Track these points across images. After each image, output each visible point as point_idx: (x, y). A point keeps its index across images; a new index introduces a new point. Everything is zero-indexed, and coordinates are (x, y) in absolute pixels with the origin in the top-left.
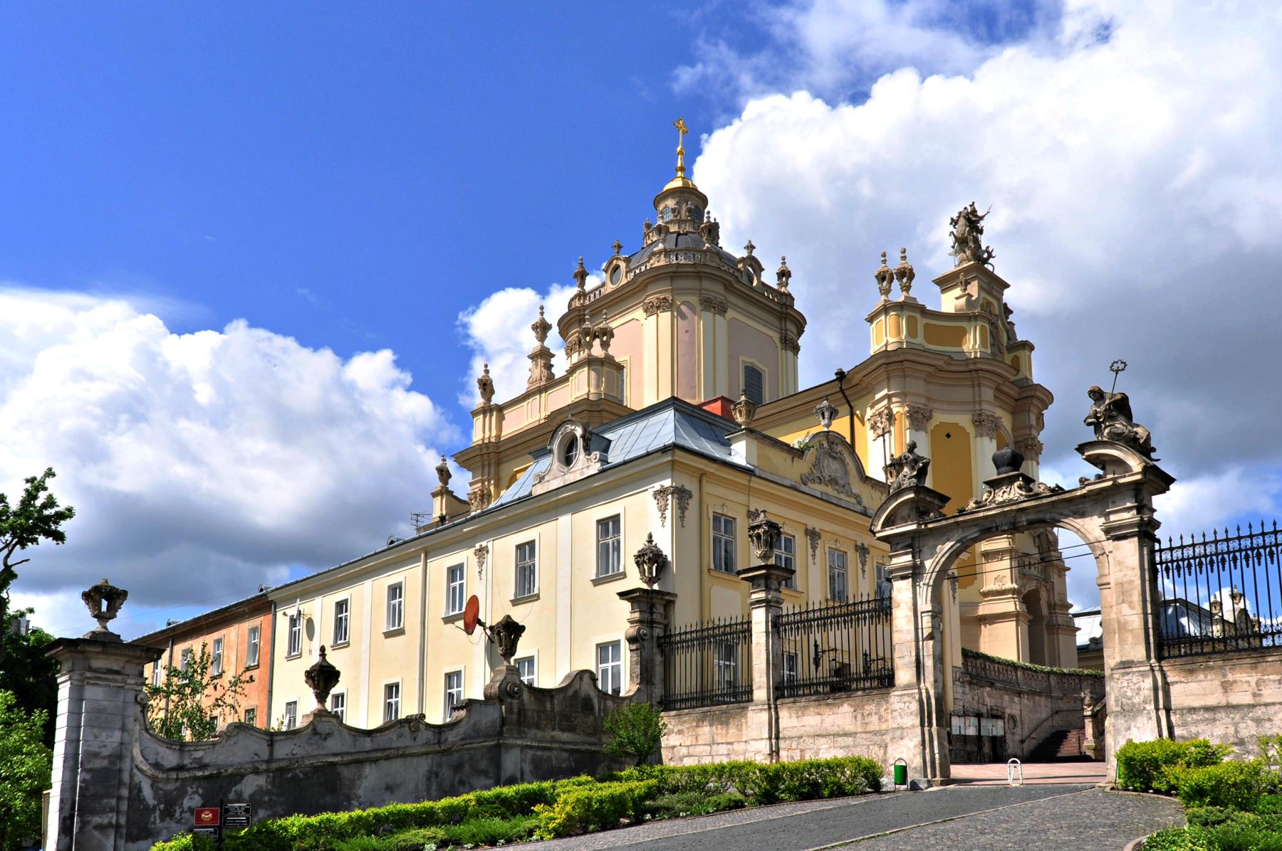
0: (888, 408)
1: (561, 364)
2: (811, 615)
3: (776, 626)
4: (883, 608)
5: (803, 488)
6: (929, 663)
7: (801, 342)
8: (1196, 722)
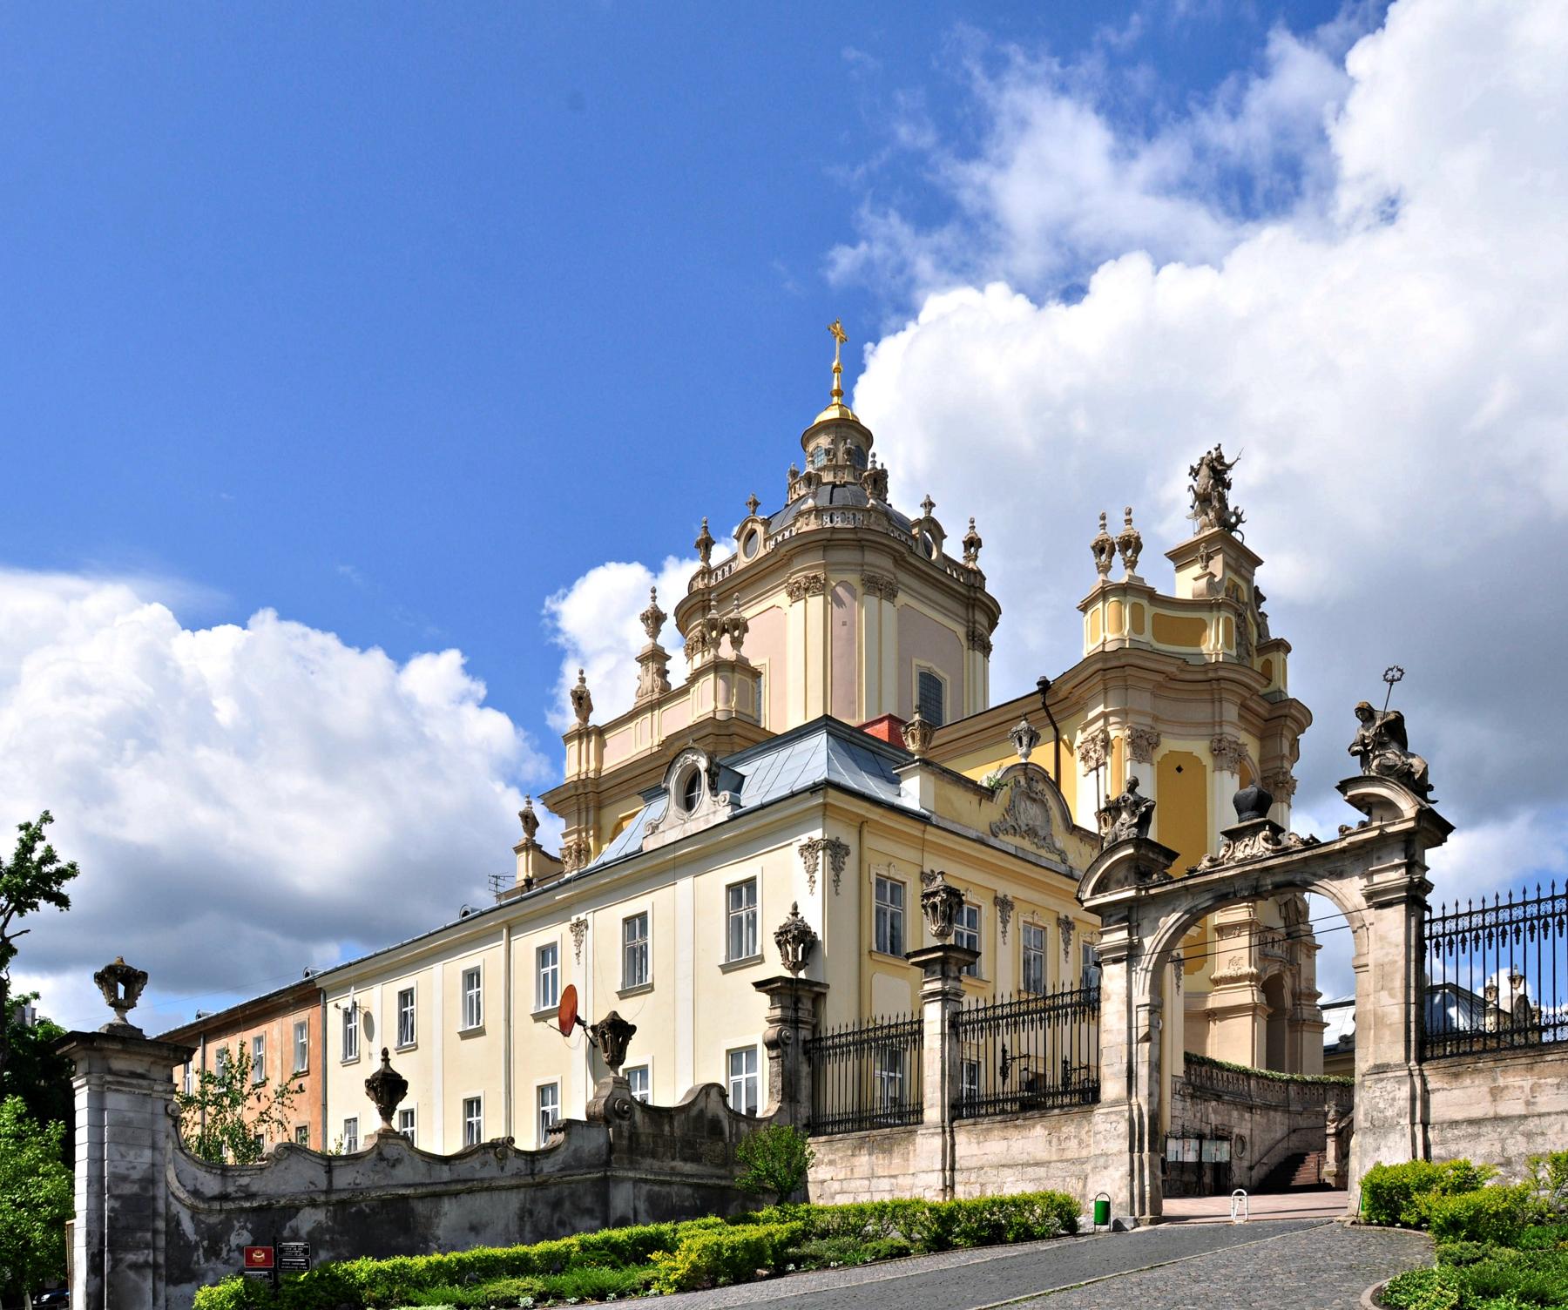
0: (1105, 731)
1: (679, 670)
2: (999, 1012)
3: (955, 1026)
4: (1088, 1002)
5: (992, 841)
6: (1143, 1071)
7: (993, 639)
8: (1457, 1139)
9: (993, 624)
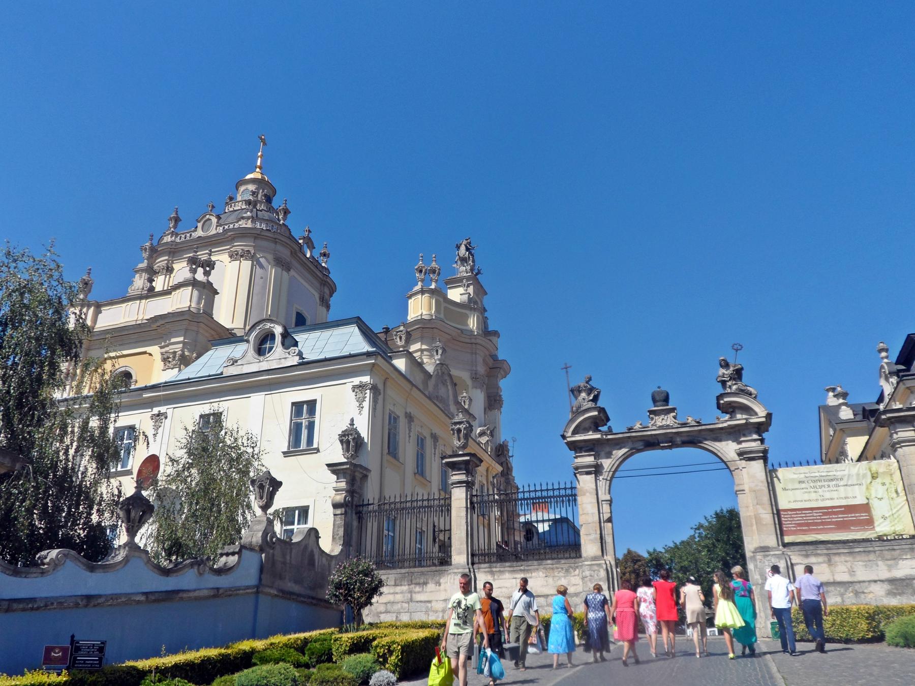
6: (609, 539)
9: (331, 296)
